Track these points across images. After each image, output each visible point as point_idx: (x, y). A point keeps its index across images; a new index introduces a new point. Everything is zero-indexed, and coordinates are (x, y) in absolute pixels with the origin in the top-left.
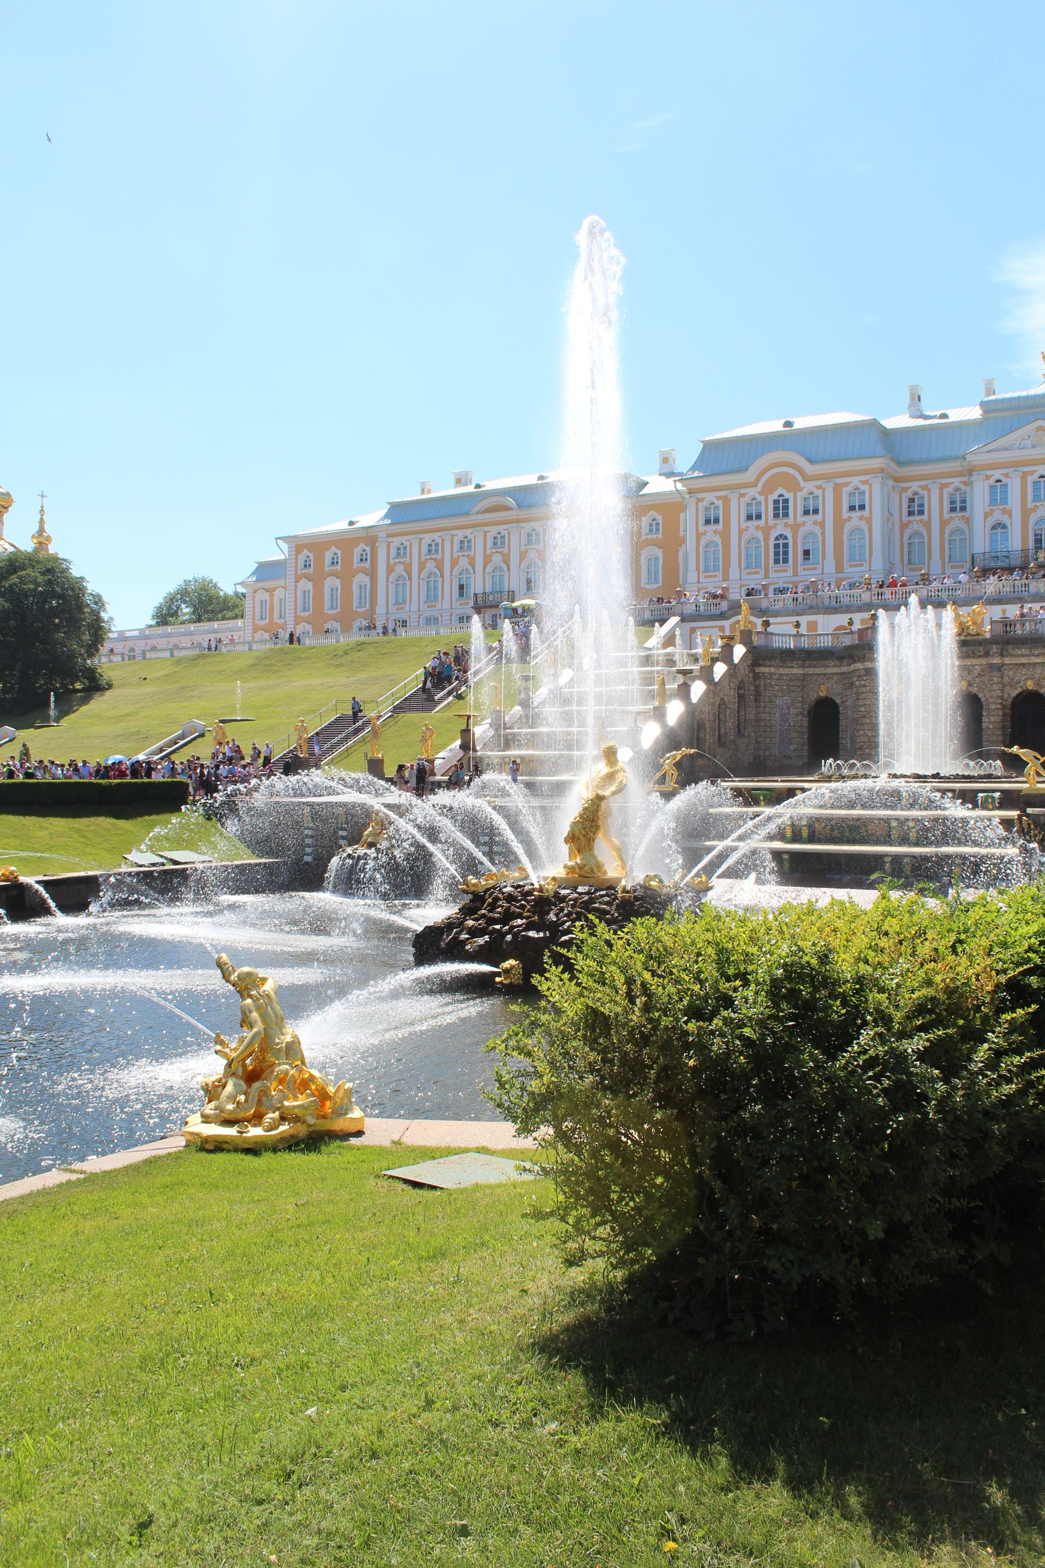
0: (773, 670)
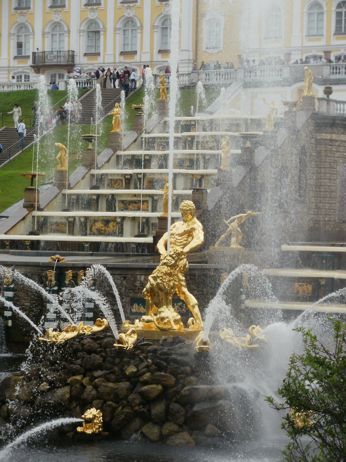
0: (334, 137)
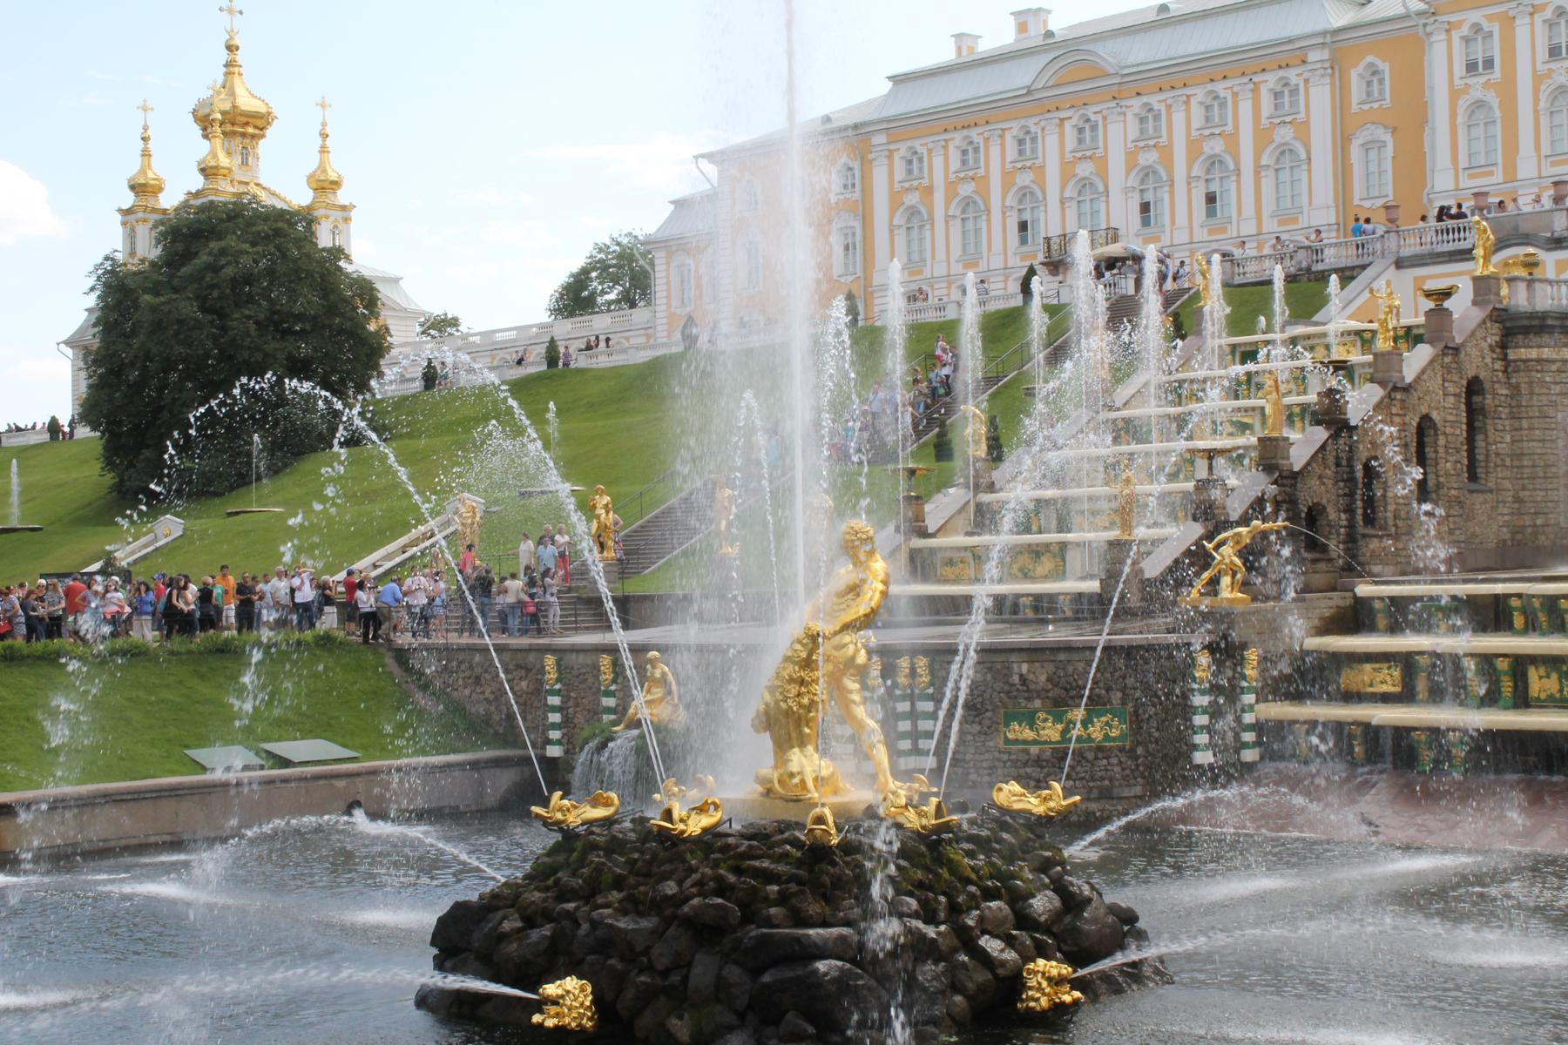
0: (1546, 353)
